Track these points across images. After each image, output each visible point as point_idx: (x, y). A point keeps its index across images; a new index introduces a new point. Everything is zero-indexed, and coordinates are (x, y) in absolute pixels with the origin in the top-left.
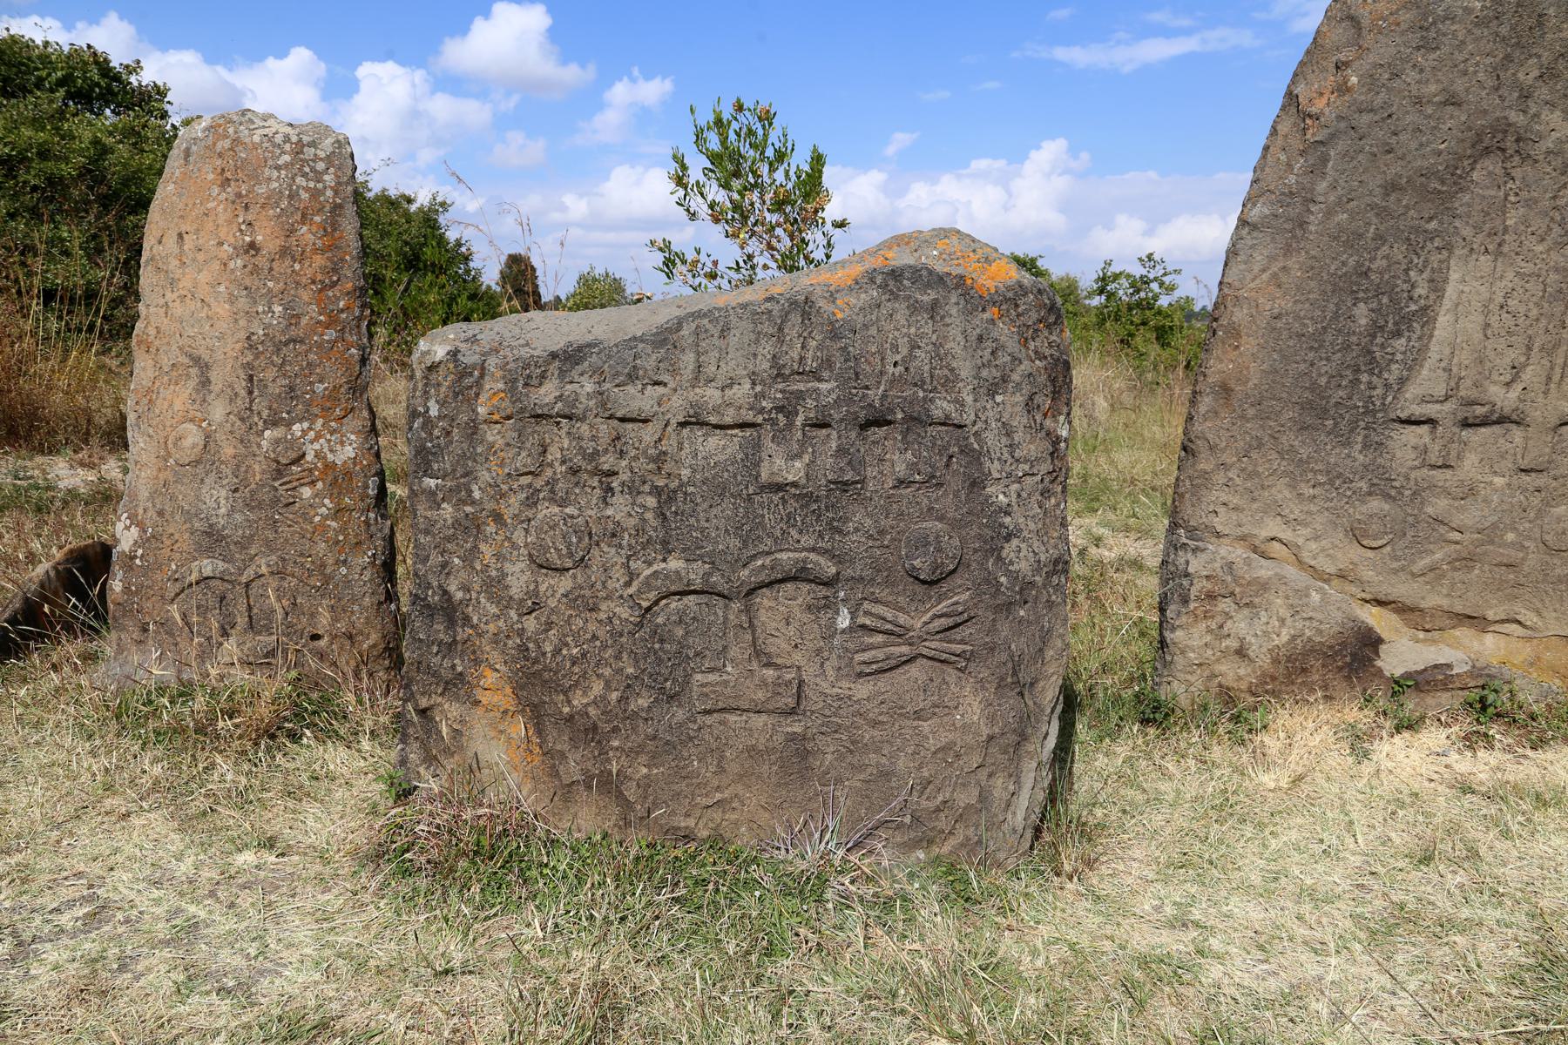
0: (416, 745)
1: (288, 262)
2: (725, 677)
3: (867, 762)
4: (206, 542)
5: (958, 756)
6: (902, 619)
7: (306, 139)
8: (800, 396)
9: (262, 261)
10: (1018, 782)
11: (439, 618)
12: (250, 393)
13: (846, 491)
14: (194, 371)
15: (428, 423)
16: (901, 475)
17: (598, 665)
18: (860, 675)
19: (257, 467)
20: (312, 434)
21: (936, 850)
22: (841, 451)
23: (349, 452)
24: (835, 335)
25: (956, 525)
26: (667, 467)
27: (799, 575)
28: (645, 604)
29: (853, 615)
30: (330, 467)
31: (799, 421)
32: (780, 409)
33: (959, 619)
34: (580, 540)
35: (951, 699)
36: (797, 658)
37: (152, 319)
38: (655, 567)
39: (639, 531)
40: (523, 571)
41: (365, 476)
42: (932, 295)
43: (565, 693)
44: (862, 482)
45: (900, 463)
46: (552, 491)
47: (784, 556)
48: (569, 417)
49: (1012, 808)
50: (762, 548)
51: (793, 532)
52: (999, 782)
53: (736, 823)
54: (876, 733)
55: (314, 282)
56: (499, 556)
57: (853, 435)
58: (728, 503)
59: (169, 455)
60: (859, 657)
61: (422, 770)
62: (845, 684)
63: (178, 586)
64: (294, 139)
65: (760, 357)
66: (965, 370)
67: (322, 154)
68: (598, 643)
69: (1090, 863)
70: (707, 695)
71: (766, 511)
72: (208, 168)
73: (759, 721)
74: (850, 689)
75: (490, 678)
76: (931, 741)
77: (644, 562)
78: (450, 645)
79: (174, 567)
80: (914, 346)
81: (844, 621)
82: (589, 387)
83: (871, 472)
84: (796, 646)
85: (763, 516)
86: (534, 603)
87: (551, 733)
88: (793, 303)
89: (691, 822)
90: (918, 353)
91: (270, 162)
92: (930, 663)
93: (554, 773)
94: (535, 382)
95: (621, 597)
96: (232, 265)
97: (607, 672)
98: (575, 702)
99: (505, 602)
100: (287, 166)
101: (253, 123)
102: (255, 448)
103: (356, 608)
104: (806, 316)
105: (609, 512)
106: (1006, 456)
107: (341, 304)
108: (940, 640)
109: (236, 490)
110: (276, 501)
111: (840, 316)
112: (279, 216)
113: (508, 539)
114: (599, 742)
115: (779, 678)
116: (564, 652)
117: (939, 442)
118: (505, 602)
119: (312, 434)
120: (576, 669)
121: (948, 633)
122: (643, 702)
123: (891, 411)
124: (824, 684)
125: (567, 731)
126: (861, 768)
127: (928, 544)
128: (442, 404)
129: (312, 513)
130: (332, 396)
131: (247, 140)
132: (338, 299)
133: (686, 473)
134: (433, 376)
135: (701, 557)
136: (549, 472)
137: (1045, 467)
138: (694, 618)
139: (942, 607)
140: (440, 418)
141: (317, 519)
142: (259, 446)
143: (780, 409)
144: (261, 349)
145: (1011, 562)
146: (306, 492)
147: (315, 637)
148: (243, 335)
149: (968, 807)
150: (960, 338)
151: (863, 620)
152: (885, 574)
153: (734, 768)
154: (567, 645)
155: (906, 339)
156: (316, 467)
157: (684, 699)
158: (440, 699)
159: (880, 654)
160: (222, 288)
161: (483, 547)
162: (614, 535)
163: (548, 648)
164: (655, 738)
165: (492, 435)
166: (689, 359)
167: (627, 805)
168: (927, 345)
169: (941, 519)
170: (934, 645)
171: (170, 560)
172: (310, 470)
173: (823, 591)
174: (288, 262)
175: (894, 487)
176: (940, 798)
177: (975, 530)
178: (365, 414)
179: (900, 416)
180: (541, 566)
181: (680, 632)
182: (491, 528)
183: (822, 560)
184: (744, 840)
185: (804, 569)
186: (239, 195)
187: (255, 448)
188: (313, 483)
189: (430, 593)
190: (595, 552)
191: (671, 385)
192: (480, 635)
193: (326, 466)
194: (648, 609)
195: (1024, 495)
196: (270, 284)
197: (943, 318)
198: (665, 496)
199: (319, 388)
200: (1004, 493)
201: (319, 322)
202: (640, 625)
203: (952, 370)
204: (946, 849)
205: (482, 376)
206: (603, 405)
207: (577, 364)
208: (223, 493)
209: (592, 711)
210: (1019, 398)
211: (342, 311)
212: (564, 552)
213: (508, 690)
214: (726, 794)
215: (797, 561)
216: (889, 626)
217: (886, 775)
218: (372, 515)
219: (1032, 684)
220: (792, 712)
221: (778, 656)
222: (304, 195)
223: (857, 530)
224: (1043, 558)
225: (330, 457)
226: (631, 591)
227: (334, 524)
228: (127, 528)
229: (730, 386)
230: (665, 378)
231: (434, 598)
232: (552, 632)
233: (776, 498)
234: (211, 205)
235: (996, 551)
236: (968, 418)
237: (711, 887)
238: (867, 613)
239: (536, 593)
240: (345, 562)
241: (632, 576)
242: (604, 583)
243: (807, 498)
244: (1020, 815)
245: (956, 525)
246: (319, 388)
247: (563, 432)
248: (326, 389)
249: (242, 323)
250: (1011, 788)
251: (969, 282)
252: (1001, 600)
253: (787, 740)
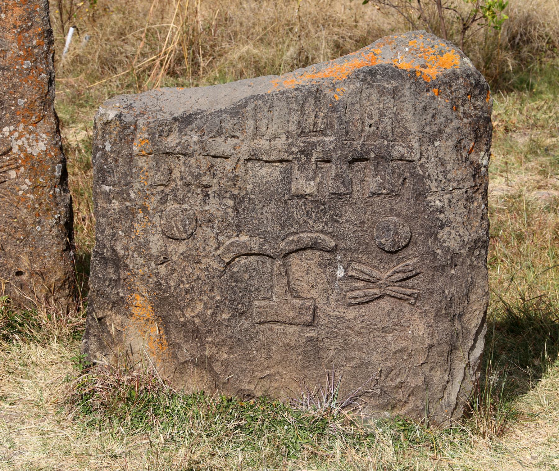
0: (94, 340)
2: (272, 303)
3: (354, 356)
5: (410, 356)
6: (375, 273)
8: (314, 144)
10: (451, 373)
11: (110, 265)
13: (341, 199)
15: (105, 155)
16: (374, 190)
17: (200, 294)
18: (350, 305)
20: (16, 134)
21: (396, 412)
22: (337, 176)
23: (42, 146)
24: (334, 109)
25: (407, 219)
26: (239, 184)
27: (313, 246)
28: (227, 260)
29: (346, 270)
30: (29, 157)
31: (313, 159)
32: (302, 152)
33: (410, 274)
34: (191, 223)
35: (405, 322)
36: (313, 293)
38: (232, 240)
39: (223, 219)
40: (158, 240)
41: (53, 163)
42: (394, 84)
43: (182, 310)
44: (351, 193)
45: (372, 183)
46: (175, 195)
47: (305, 235)
48: (185, 155)
49: (447, 391)
50: (292, 230)
51: (311, 222)
52: (438, 373)
53: (278, 388)
54: (359, 339)
55: (15, 27)
56: (145, 231)
57: (345, 167)
58: (273, 204)
60: (349, 294)
61: (98, 354)
62: (341, 310)
65: (291, 123)
66: (414, 128)
68: (200, 282)
69: (501, 432)
70: (261, 313)
71: (295, 209)
73: (291, 329)
74: (344, 312)
75: (139, 300)
76: (393, 346)
77: (226, 237)
78: (116, 281)
80: (382, 115)
81: (340, 273)
82: (196, 138)
83: (356, 188)
84: (312, 287)
85: (293, 212)
86: (164, 258)
87: (173, 332)
88: (310, 92)
89: (252, 387)
90: (384, 119)
92: (392, 299)
93: (175, 357)
94: (165, 134)
95: (213, 256)
97: (205, 298)
98: (187, 315)
99: (148, 257)
103: (47, 254)
104: (317, 99)
105: (207, 208)
106: (441, 177)
107: (35, 42)
108: (399, 286)
111: (337, 98)
113: (150, 221)
114: (200, 339)
115: (302, 304)
116: (181, 286)
117: (397, 171)
118: (148, 257)
119: (16, 134)
120: (188, 296)
121: (404, 282)
122: (225, 316)
123: (367, 153)
124: (329, 309)
125: (183, 332)
126: (351, 359)
127: (389, 230)
128: (113, 144)
129: (17, 189)
130: (30, 107)
132: (32, 39)
133: (249, 187)
134: (108, 128)
135: (258, 235)
136: (173, 185)
137: (471, 183)
138: (254, 269)
139: (400, 267)
140: (111, 152)
141: (21, 193)
143: (302, 152)
145: (444, 241)
146: (13, 174)
147: (19, 273)
149: (417, 387)
150: (411, 109)
151: (351, 273)
152: (364, 247)
153: (276, 356)
154: (183, 282)
155: (377, 111)
156: (20, 157)
157: (248, 315)
158: (109, 312)
159: (361, 293)
161: (136, 225)
162: (209, 221)
163: (172, 284)
164: (232, 337)
165: (141, 162)
166: (250, 124)
167: (215, 375)
168: (390, 114)
169: (398, 215)
170: (394, 289)
172: (16, 159)
173: (328, 256)
175: (369, 197)
176: (399, 380)
177: (420, 222)
178: (53, 119)
179: (373, 156)
180: (169, 237)
181: (246, 277)
182: (140, 215)
183: (327, 238)
184: (282, 400)
185: (316, 243)
188: (18, 168)
189: (105, 251)
190: (199, 230)
191: (241, 138)
192: (134, 276)
193: (27, 156)
194: (229, 263)
195: (454, 201)
197: (400, 97)
198: (238, 200)
199: (21, 102)
200: (440, 200)
201: (20, 56)
202: (224, 272)
203: (406, 128)
204: (403, 412)
205: (135, 129)
206: (203, 148)
207: (189, 125)
209: (197, 320)
210: (451, 143)
211: (35, 47)
212: (182, 229)
213: (149, 308)
214: (272, 371)
215: (312, 238)
216: (367, 277)
217: (365, 364)
218: (57, 190)
219: (460, 316)
220: (310, 325)
221: (302, 292)
223: (347, 221)
224: (466, 239)
225: (29, 150)
226: (219, 252)
227: (32, 196)
229: (274, 139)
230: (237, 134)
231: (107, 254)
232: (175, 275)
233: (300, 202)
235: (434, 235)
236: (416, 156)
237: (260, 423)
238: (354, 269)
239: (166, 252)
240: (39, 222)
241: (219, 244)
242: (204, 248)
243: (318, 203)
244: (453, 397)
245: (407, 219)
246: (21, 102)
247: (181, 162)
248: (25, 103)
250: (446, 378)
251: (418, 74)
252: (437, 263)
253: (307, 341)
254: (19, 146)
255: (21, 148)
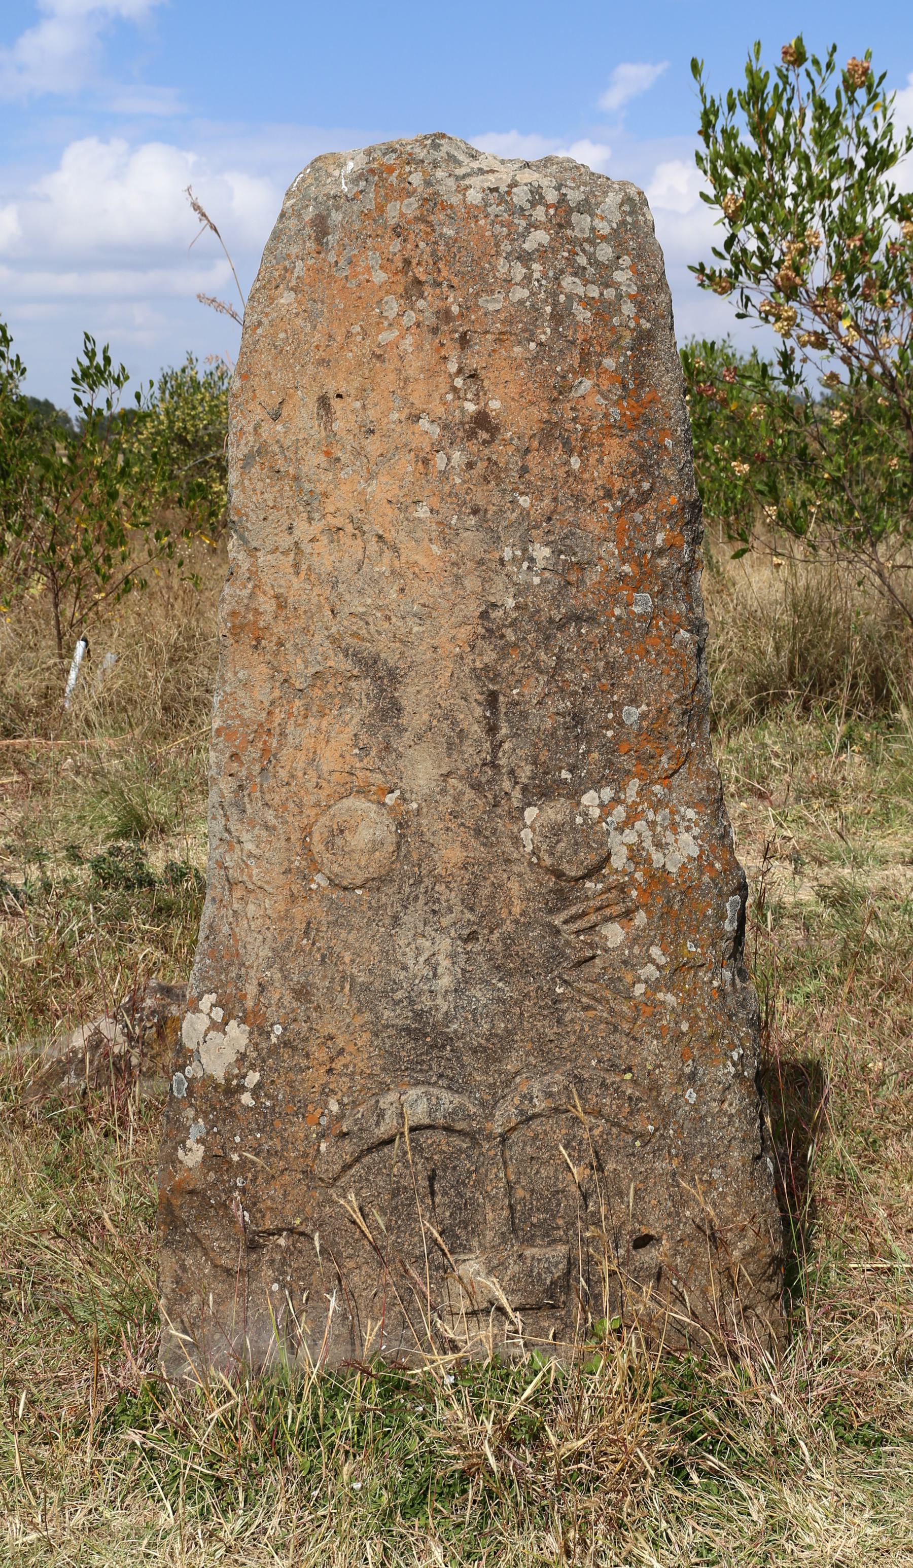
1: (557, 456)
4: (407, 1049)
7: (574, 196)
9: (503, 453)
12: (492, 729)
14: (361, 687)
19: (514, 886)
20: (620, 812)
37: (266, 578)
41: (720, 894)
55: (608, 495)
59: (315, 865)
63: (348, 1148)
64: (552, 197)
67: (604, 228)
72: (373, 258)
79: (334, 1107)
91: (506, 247)
96: (440, 461)
100: (542, 253)
101: (459, 164)
102: (508, 847)
107: (660, 538)
109: (472, 937)
110: (555, 956)
112: (536, 359)
119: (620, 812)
129: (629, 978)
131: (455, 200)
132: (653, 529)
141: (640, 989)
142: (517, 841)
144: (510, 636)
146: (614, 934)
147: (642, 1242)
148: (473, 609)
156: (633, 880)
160: (422, 512)
171: (326, 1092)
172: (622, 889)
174: (557, 456)
186: (445, 315)
187: (508, 847)
188: (628, 915)
193: (651, 877)
196: (524, 501)
199: (632, 714)
201: (623, 577)
208: (445, 944)
211: (660, 552)
218: (727, 975)
222: (583, 315)
225: (657, 858)
227: (670, 999)
228: (220, 1027)
234: (386, 337)
246: (632, 714)
248: (643, 716)
249: (471, 583)
254: (630, 847)
255: (635, 854)
